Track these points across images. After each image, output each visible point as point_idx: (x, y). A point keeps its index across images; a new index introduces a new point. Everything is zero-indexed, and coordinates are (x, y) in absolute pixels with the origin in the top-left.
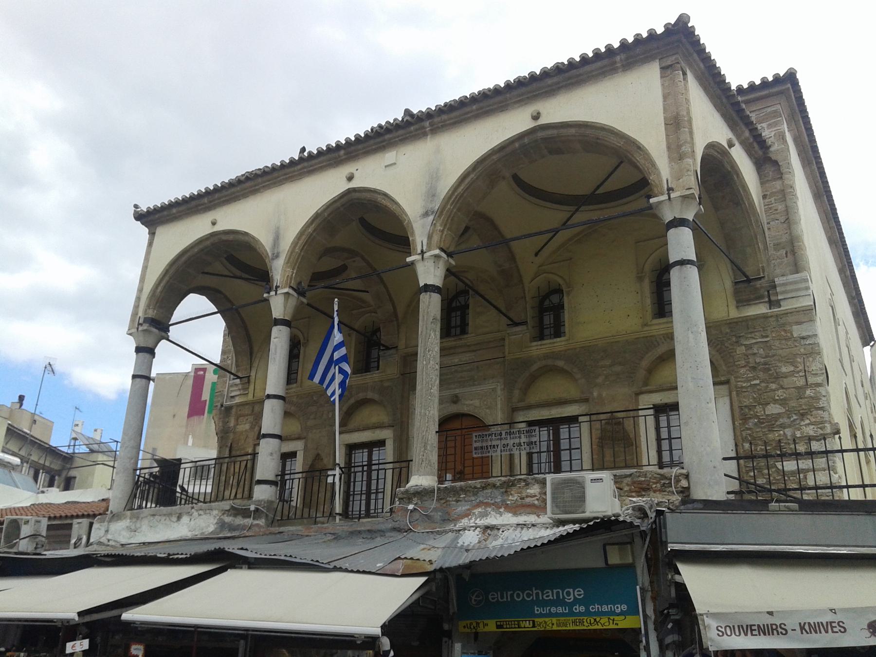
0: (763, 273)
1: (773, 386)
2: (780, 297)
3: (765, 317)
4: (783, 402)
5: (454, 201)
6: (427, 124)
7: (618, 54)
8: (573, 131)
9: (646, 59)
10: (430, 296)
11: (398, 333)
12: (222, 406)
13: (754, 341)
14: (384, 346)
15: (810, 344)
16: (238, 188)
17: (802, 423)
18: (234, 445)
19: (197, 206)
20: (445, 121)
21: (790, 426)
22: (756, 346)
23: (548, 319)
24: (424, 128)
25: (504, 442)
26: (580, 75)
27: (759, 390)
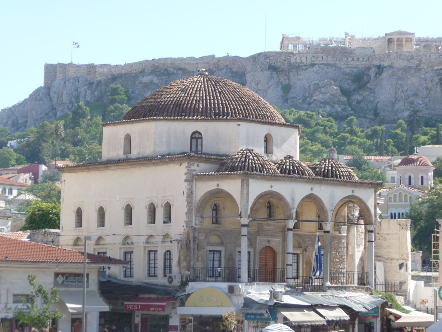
3: (338, 236)
6: (332, 182)
12: (192, 226)
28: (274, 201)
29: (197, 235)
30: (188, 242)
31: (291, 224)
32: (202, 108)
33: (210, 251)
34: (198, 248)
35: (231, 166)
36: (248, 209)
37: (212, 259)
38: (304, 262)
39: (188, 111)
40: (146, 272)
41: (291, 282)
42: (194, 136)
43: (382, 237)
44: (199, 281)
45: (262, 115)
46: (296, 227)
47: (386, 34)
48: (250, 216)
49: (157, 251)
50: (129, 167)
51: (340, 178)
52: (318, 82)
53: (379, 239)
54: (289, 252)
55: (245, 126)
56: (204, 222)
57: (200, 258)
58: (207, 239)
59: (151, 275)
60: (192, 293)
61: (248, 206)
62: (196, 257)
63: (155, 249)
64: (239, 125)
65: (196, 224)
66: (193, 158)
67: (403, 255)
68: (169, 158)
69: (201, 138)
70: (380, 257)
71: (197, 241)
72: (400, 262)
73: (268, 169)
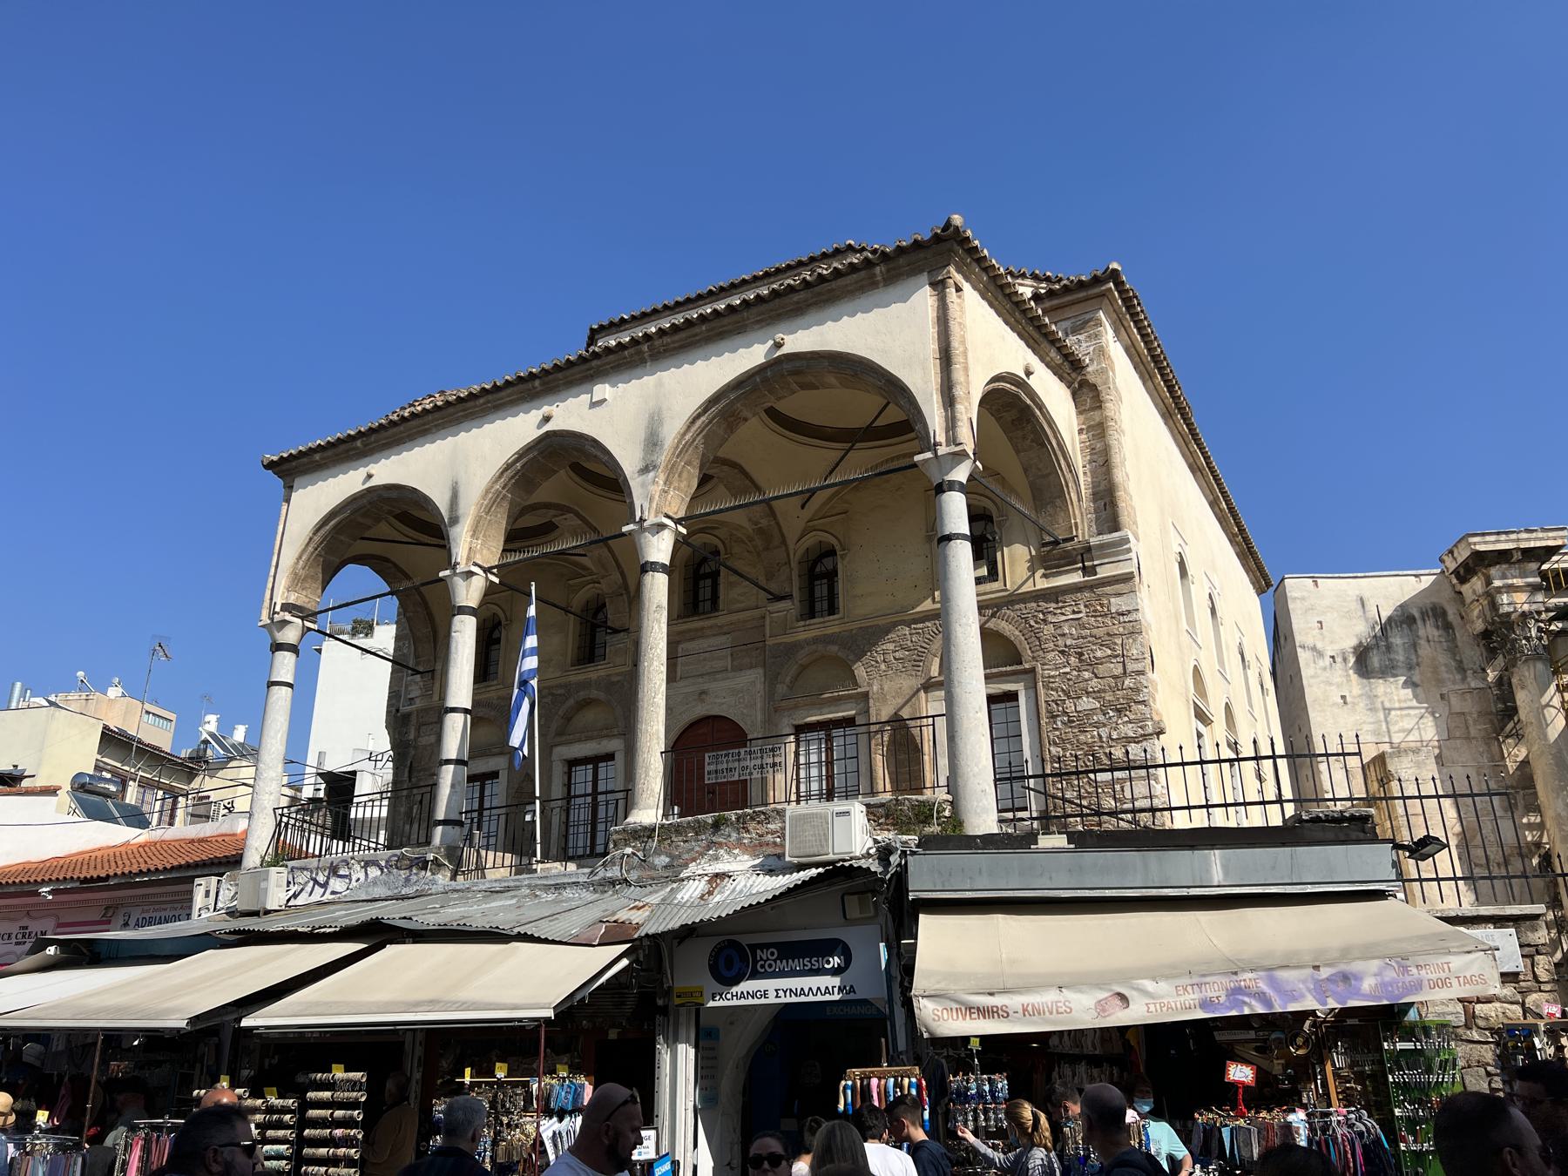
0: (1077, 530)
1: (1087, 675)
2: (1096, 563)
4: (1097, 694)
5: (681, 452)
6: (645, 348)
7: (878, 264)
9: (914, 271)
10: (653, 576)
11: (630, 610)
12: (398, 711)
13: (1064, 618)
14: (610, 628)
15: (1130, 622)
16: (402, 428)
17: (1120, 721)
18: (414, 765)
19: (348, 451)
20: (668, 344)
21: (1105, 725)
22: (1067, 624)
23: (821, 589)
24: (640, 352)
25: (742, 764)
26: (833, 290)
27: (1069, 680)
62: (402, 809)
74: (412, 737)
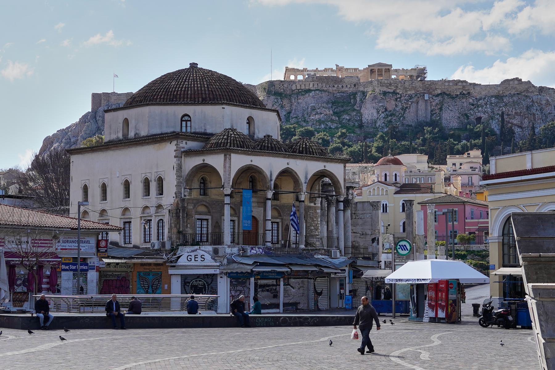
4: (314, 226)
8: (329, 173)
9: (342, 163)
28: (256, 175)
29: (186, 206)
30: (178, 211)
31: (270, 194)
32: (191, 94)
33: (198, 219)
34: (187, 216)
35: (216, 142)
36: (230, 180)
37: (200, 226)
38: (283, 229)
39: (178, 96)
40: (143, 239)
41: (269, 244)
42: (184, 119)
43: (358, 216)
44: (188, 245)
45: (244, 101)
46: (276, 197)
47: (368, 66)
48: (232, 187)
49: (151, 220)
50: (127, 147)
51: (314, 155)
52: (314, 105)
53: (355, 218)
54: (268, 219)
55: (229, 109)
56: (192, 193)
57: (189, 226)
58: (195, 209)
59: (146, 241)
60: (182, 255)
61: (230, 178)
62: (185, 224)
63: (149, 218)
64: (224, 108)
65: (185, 196)
66: (181, 137)
67: (375, 231)
68: (160, 137)
69: (190, 121)
70: (356, 233)
71: (187, 210)
72: (373, 237)
73: (248, 145)
74: (186, 206)
